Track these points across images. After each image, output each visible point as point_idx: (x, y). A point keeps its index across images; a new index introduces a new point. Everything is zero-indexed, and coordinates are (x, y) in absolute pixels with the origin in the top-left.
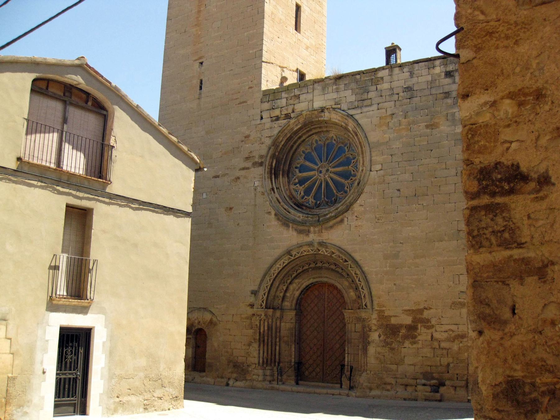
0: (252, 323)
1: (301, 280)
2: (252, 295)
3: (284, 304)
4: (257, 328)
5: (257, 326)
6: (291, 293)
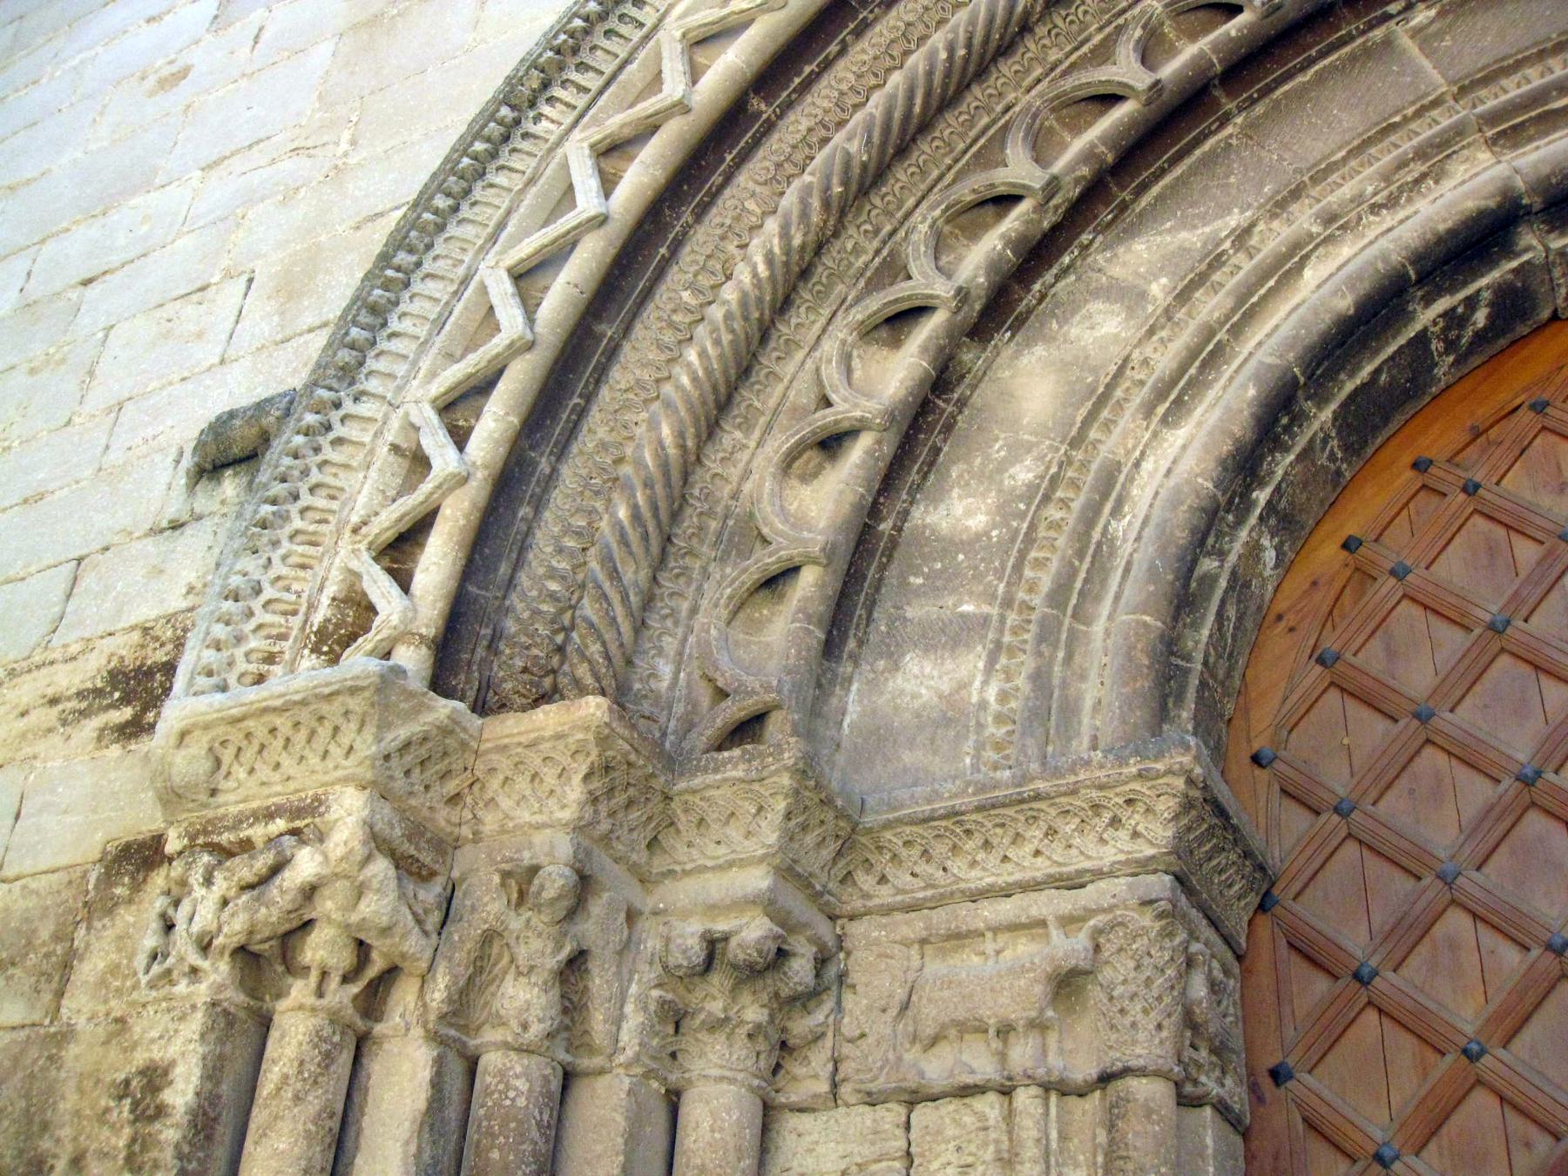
0: (66, 1036)
1: (1235, 219)
2: (202, 503)
3: (854, 705)
5: (148, 1111)
6: (1023, 474)
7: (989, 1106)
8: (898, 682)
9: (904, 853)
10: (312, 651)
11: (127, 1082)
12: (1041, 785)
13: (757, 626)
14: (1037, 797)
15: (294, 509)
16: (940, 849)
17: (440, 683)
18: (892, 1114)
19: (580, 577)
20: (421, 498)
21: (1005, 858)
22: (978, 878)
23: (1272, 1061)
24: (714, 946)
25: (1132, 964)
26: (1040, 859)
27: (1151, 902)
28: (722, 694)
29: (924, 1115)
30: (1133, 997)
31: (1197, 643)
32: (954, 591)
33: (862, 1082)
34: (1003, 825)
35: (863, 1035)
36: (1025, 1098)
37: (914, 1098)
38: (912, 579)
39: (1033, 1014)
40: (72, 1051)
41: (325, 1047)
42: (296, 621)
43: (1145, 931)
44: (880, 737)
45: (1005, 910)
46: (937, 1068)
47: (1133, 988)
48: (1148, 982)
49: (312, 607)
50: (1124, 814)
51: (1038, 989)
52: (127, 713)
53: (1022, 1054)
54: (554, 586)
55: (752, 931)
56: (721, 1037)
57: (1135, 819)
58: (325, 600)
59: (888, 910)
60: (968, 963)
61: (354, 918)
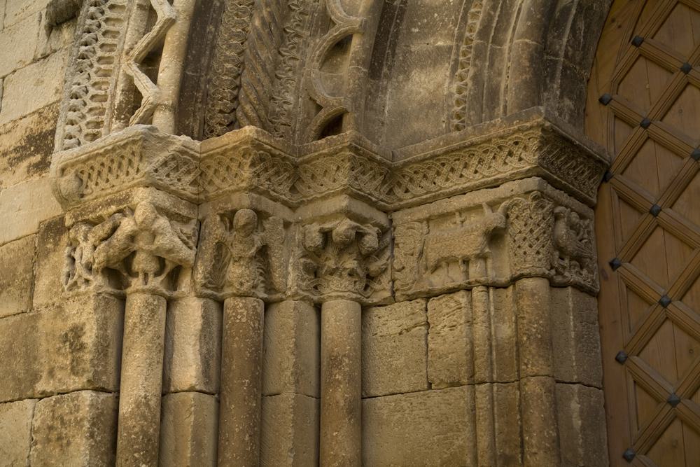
2: (54, 44)
3: (388, 101)
4: (74, 371)
7: (461, 297)
8: (409, 86)
9: (415, 176)
10: (116, 119)
11: (66, 334)
12: (474, 139)
13: (335, 68)
14: (472, 145)
15: (96, 46)
16: (431, 174)
17: (180, 129)
18: (419, 304)
19: (241, 59)
20: (155, 34)
21: (461, 176)
22: (449, 186)
23: (610, 258)
24: (326, 235)
25: (524, 223)
26: (477, 174)
27: (530, 192)
28: (319, 108)
29: (433, 303)
30: (525, 239)
31: (561, 46)
32: (433, 34)
33: (405, 290)
34: (458, 160)
35: (403, 268)
36: (478, 293)
37: (429, 296)
38: (413, 30)
39: (478, 252)
40: (40, 324)
41: (151, 307)
42: (106, 105)
43: (529, 206)
44: (402, 116)
45: (464, 201)
46: (439, 280)
47: (524, 235)
48: (531, 231)
49: (114, 96)
50: (515, 149)
51: (480, 239)
52: (38, 158)
53: (475, 270)
54: (229, 66)
55: (342, 227)
56: (336, 277)
57: (518, 151)
58: (119, 92)
59: (410, 206)
60: (449, 230)
61: (154, 247)
